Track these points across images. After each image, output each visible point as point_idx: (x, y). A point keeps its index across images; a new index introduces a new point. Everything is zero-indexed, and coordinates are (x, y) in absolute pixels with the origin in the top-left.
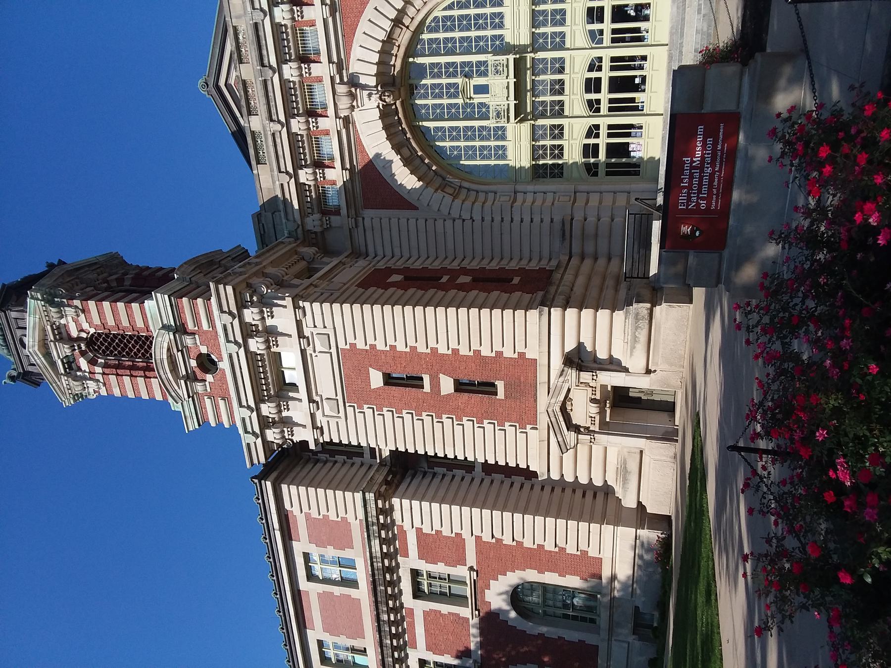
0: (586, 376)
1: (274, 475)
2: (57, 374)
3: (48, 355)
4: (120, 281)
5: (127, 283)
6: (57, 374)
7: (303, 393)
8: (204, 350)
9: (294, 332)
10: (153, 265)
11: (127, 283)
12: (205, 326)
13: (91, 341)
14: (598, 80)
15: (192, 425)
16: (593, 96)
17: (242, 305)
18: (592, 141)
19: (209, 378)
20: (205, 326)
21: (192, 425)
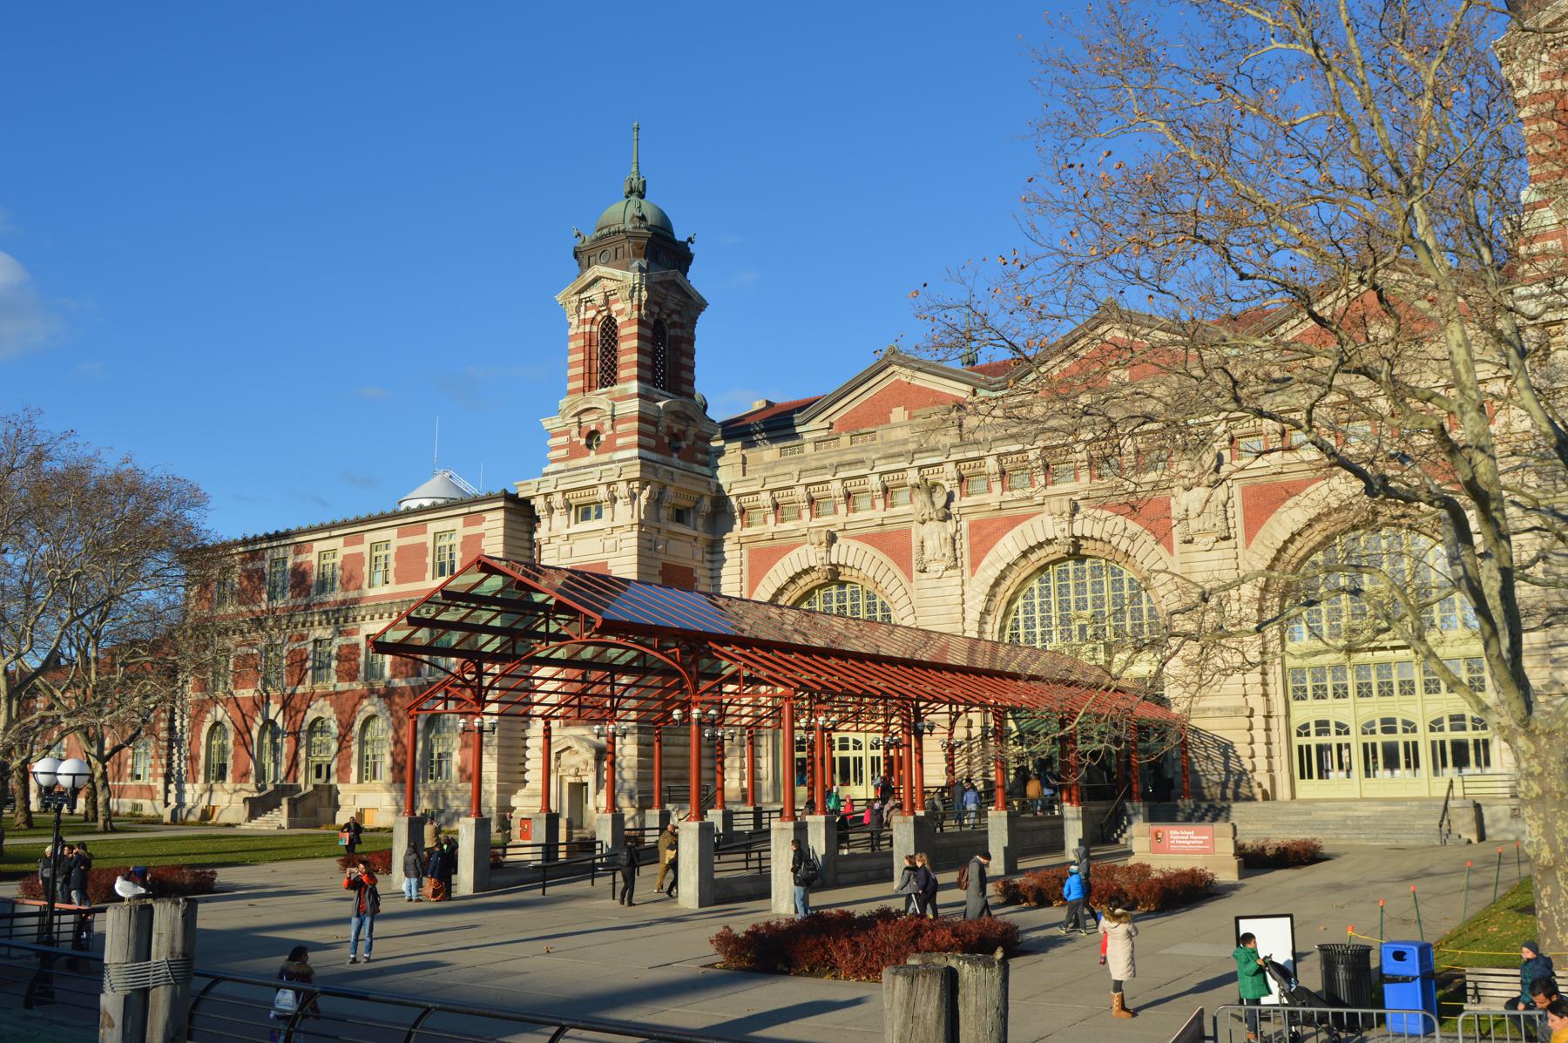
0: (592, 762)
1: (510, 505)
2: (580, 292)
3: (596, 280)
4: (674, 325)
5: (672, 332)
6: (580, 292)
7: (575, 528)
8: (603, 438)
9: (615, 524)
10: (697, 345)
11: (672, 332)
12: (620, 441)
13: (609, 317)
14: (1394, 731)
15: (547, 424)
16: (1313, 729)
17: (629, 481)
18: (1333, 728)
19: (583, 441)
20: (620, 441)
21: (547, 424)
